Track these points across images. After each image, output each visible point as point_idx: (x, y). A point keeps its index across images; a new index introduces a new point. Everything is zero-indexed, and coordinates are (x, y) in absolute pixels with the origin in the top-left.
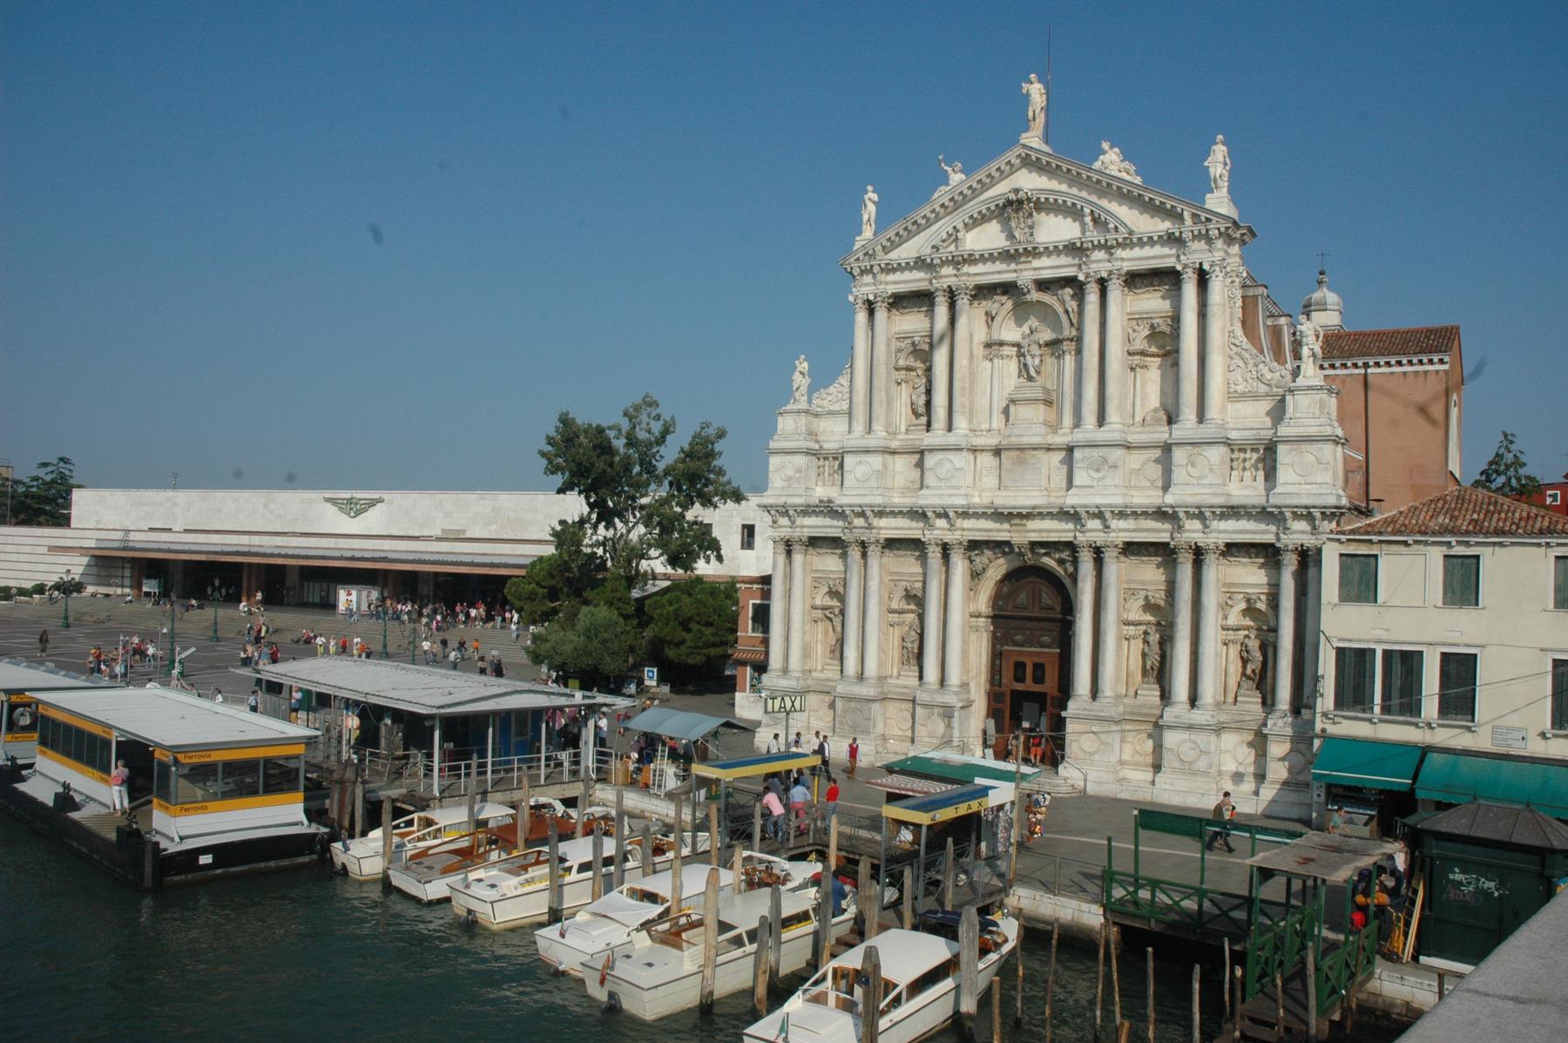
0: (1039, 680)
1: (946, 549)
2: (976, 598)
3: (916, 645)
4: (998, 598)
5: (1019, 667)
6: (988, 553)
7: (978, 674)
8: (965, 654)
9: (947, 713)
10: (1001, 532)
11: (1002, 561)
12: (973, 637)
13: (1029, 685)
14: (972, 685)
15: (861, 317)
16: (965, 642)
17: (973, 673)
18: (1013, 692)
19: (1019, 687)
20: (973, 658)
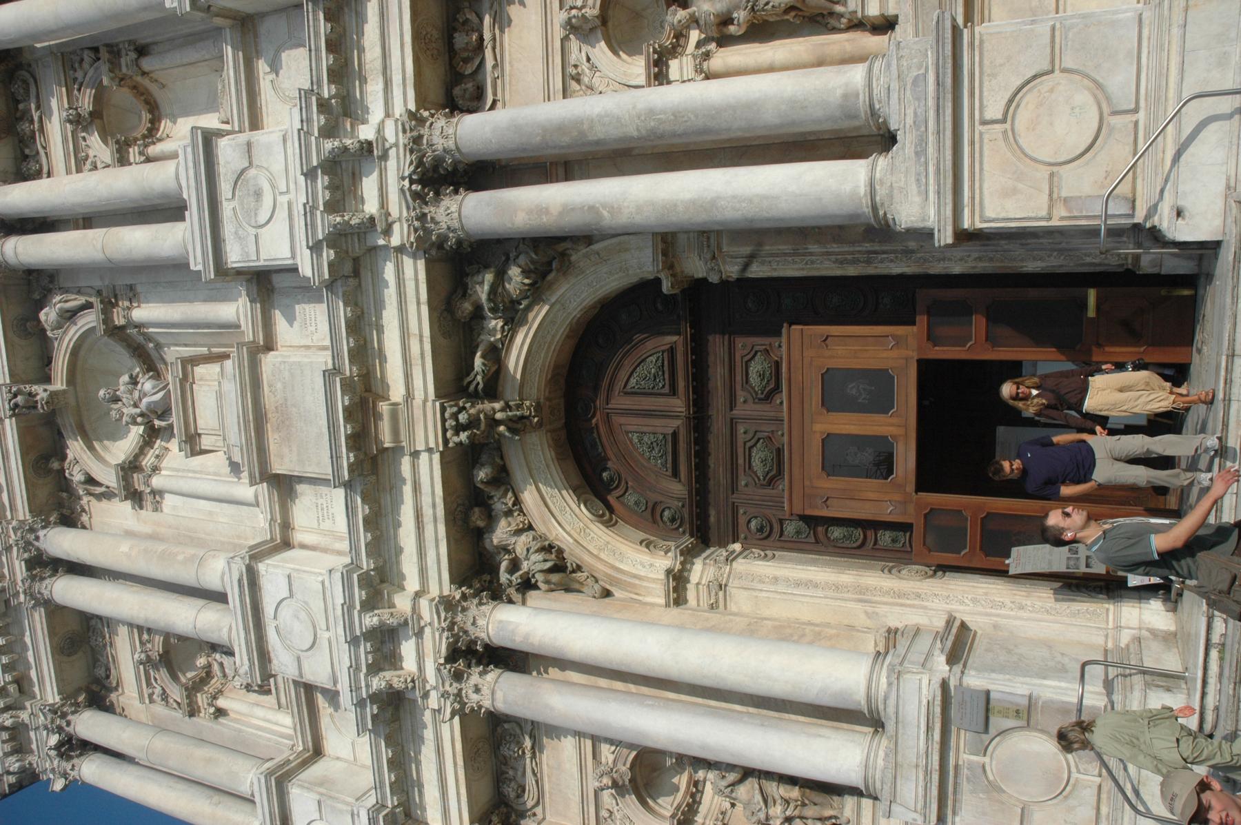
0: (876, 391)
1: (472, 654)
2: (631, 583)
3: (778, 791)
4: (653, 521)
5: (839, 457)
6: (501, 533)
7: (862, 596)
8: (788, 633)
9: (964, 716)
10: (423, 485)
11: (529, 497)
12: (740, 600)
13: (898, 426)
14: (897, 617)
15: (91, 770)
16: (753, 630)
17: (856, 612)
18: (925, 481)
19: (906, 460)
20: (804, 608)
